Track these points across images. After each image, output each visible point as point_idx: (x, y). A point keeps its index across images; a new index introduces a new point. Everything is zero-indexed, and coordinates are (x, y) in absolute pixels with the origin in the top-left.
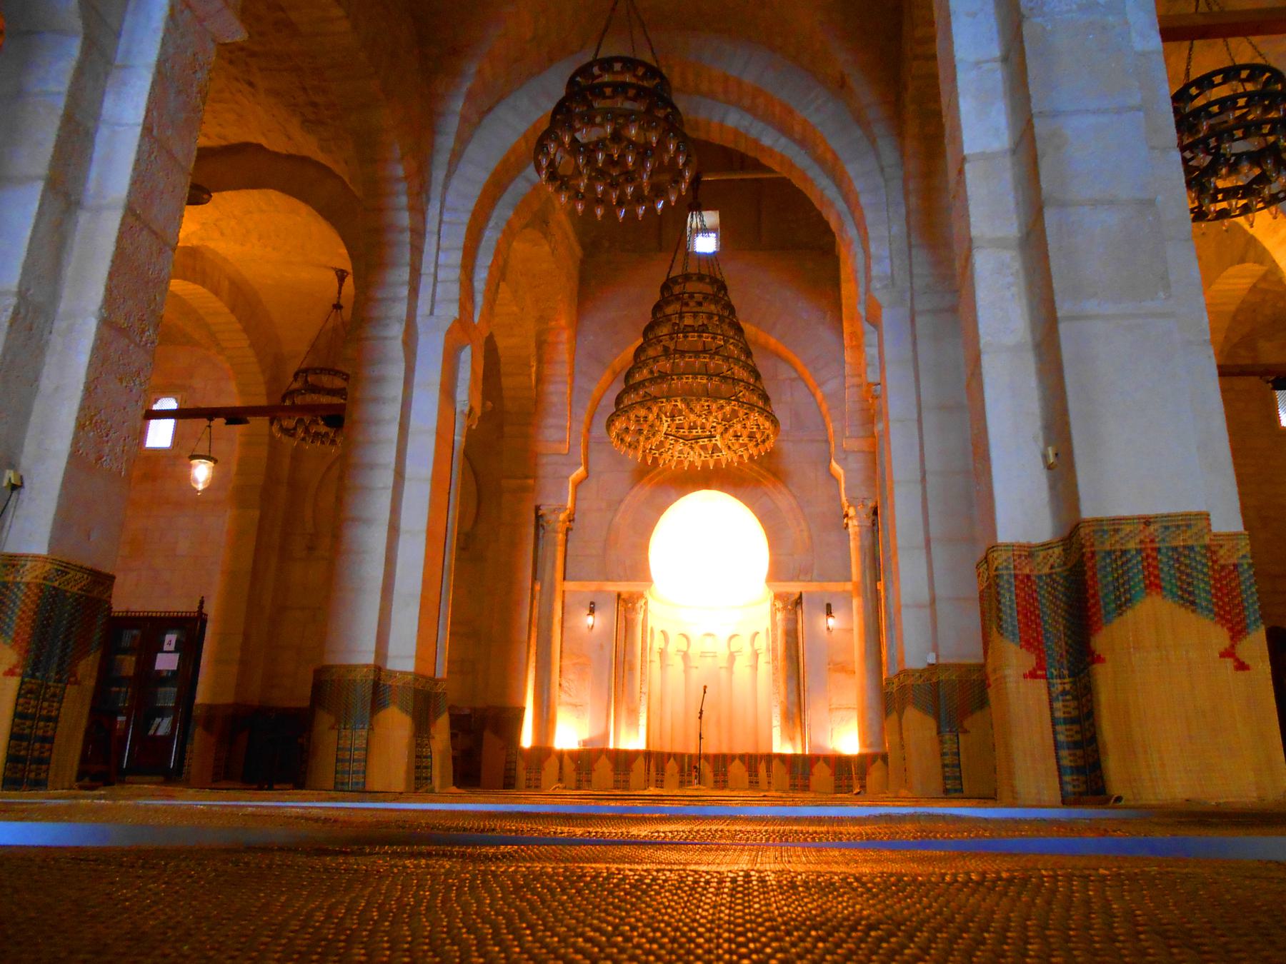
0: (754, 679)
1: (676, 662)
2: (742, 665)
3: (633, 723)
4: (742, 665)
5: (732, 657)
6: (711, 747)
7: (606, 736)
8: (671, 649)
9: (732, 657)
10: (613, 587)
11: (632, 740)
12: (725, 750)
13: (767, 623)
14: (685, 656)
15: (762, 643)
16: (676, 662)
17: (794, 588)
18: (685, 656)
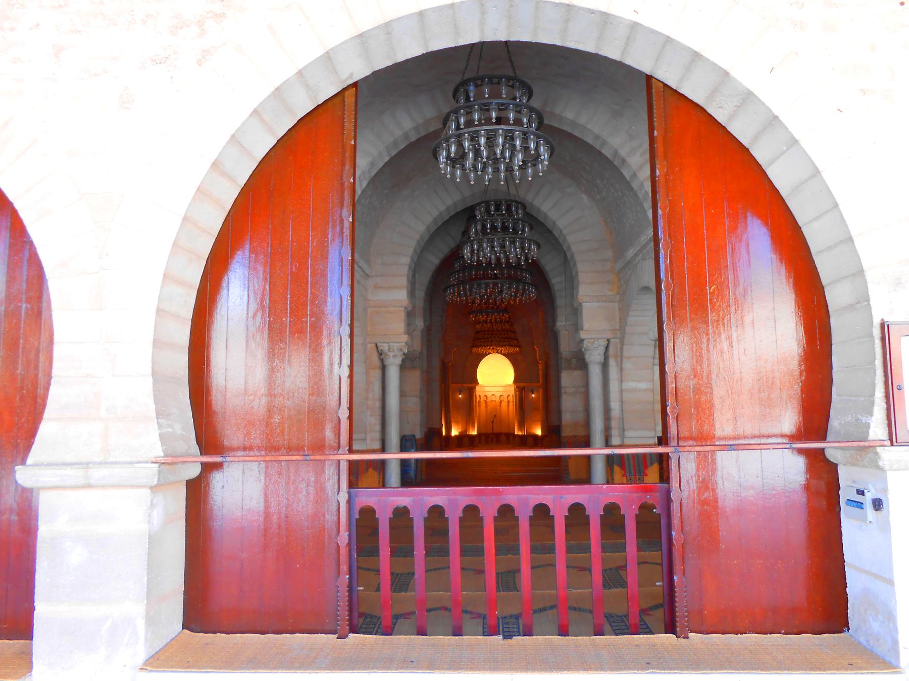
0: (509, 410)
1: (483, 405)
2: (504, 404)
3: (474, 427)
4: (504, 404)
5: (501, 402)
6: (495, 431)
7: (466, 431)
8: (482, 400)
9: (501, 402)
10: (466, 385)
11: (474, 432)
12: (499, 431)
13: (513, 393)
14: (486, 402)
15: (511, 399)
16: (483, 405)
17: (522, 385)
18: (486, 402)
